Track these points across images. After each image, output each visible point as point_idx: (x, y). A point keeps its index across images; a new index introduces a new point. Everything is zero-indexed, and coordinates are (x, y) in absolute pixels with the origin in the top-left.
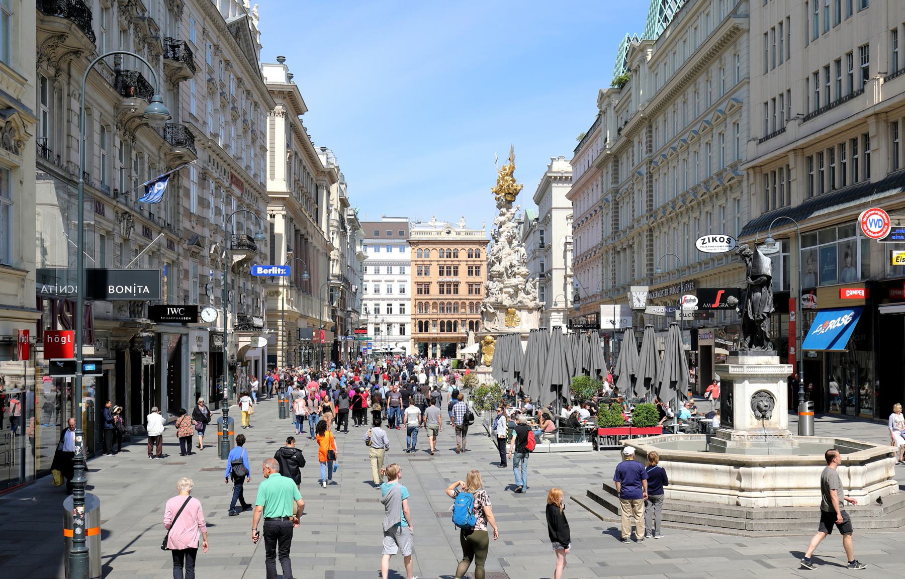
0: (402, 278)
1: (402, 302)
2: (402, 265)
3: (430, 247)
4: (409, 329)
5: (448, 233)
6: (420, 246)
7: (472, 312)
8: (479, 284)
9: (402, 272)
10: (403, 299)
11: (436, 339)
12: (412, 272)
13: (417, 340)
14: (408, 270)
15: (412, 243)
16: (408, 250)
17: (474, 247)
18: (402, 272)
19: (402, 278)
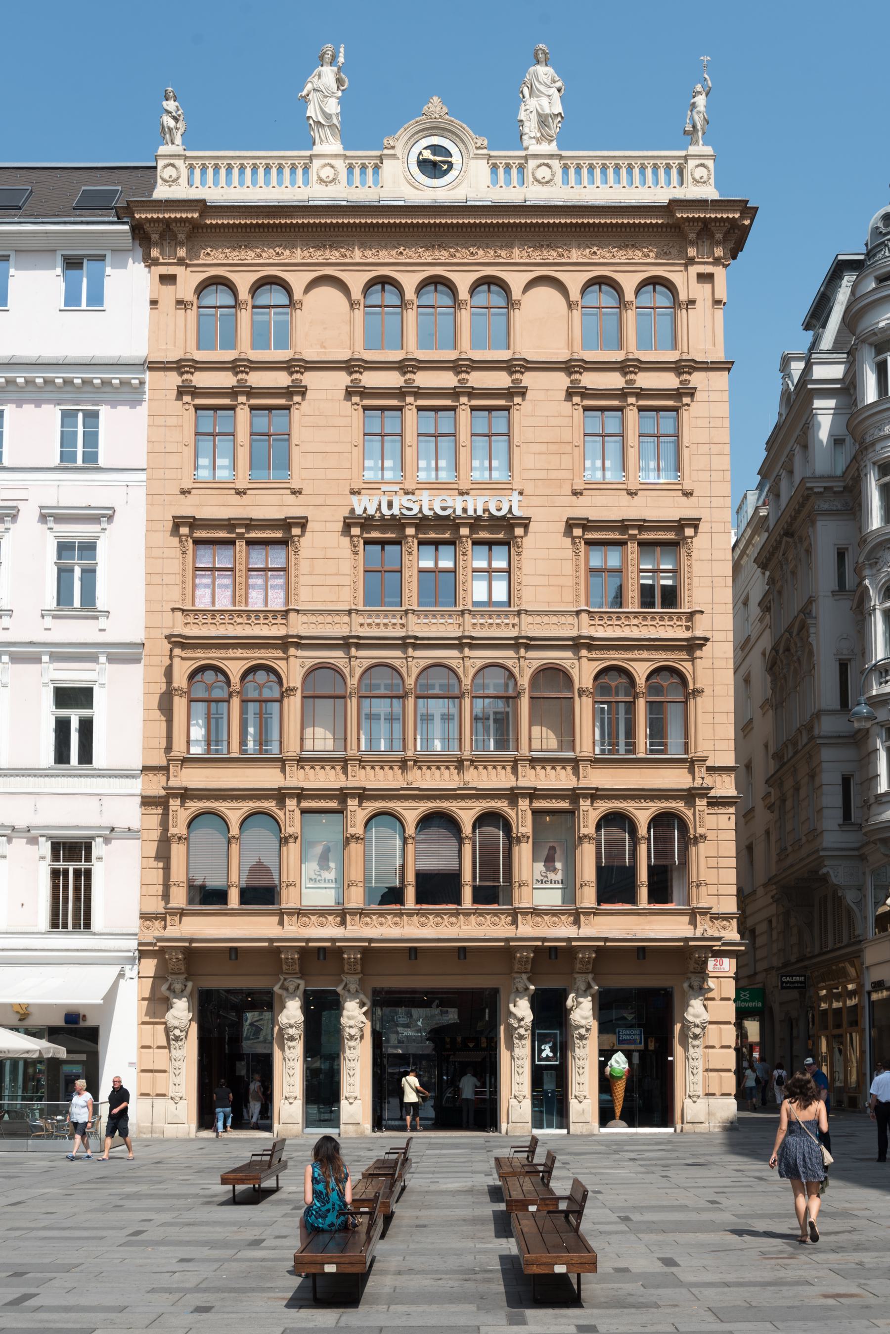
0: (77, 490)
1: (74, 675)
2: (80, 391)
3: (297, 264)
4: (120, 886)
5: (434, 167)
6: (217, 259)
7: (617, 750)
8: (671, 538)
9: (79, 451)
10: (84, 654)
11: (318, 958)
12: (154, 447)
13: (179, 968)
14: (123, 431)
15: (167, 232)
16: (130, 281)
17: (630, 268)
18: (79, 451)
19: (77, 490)
